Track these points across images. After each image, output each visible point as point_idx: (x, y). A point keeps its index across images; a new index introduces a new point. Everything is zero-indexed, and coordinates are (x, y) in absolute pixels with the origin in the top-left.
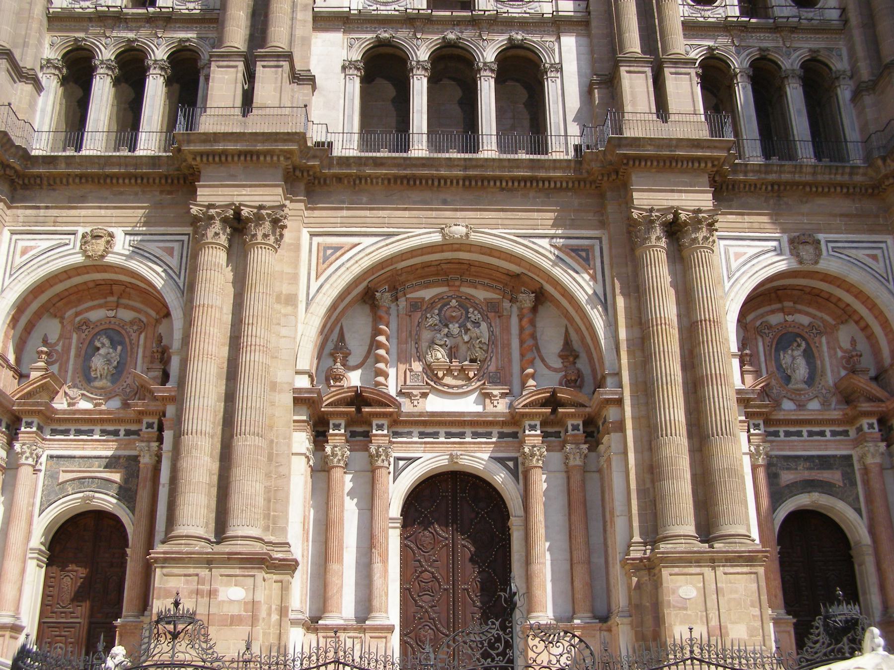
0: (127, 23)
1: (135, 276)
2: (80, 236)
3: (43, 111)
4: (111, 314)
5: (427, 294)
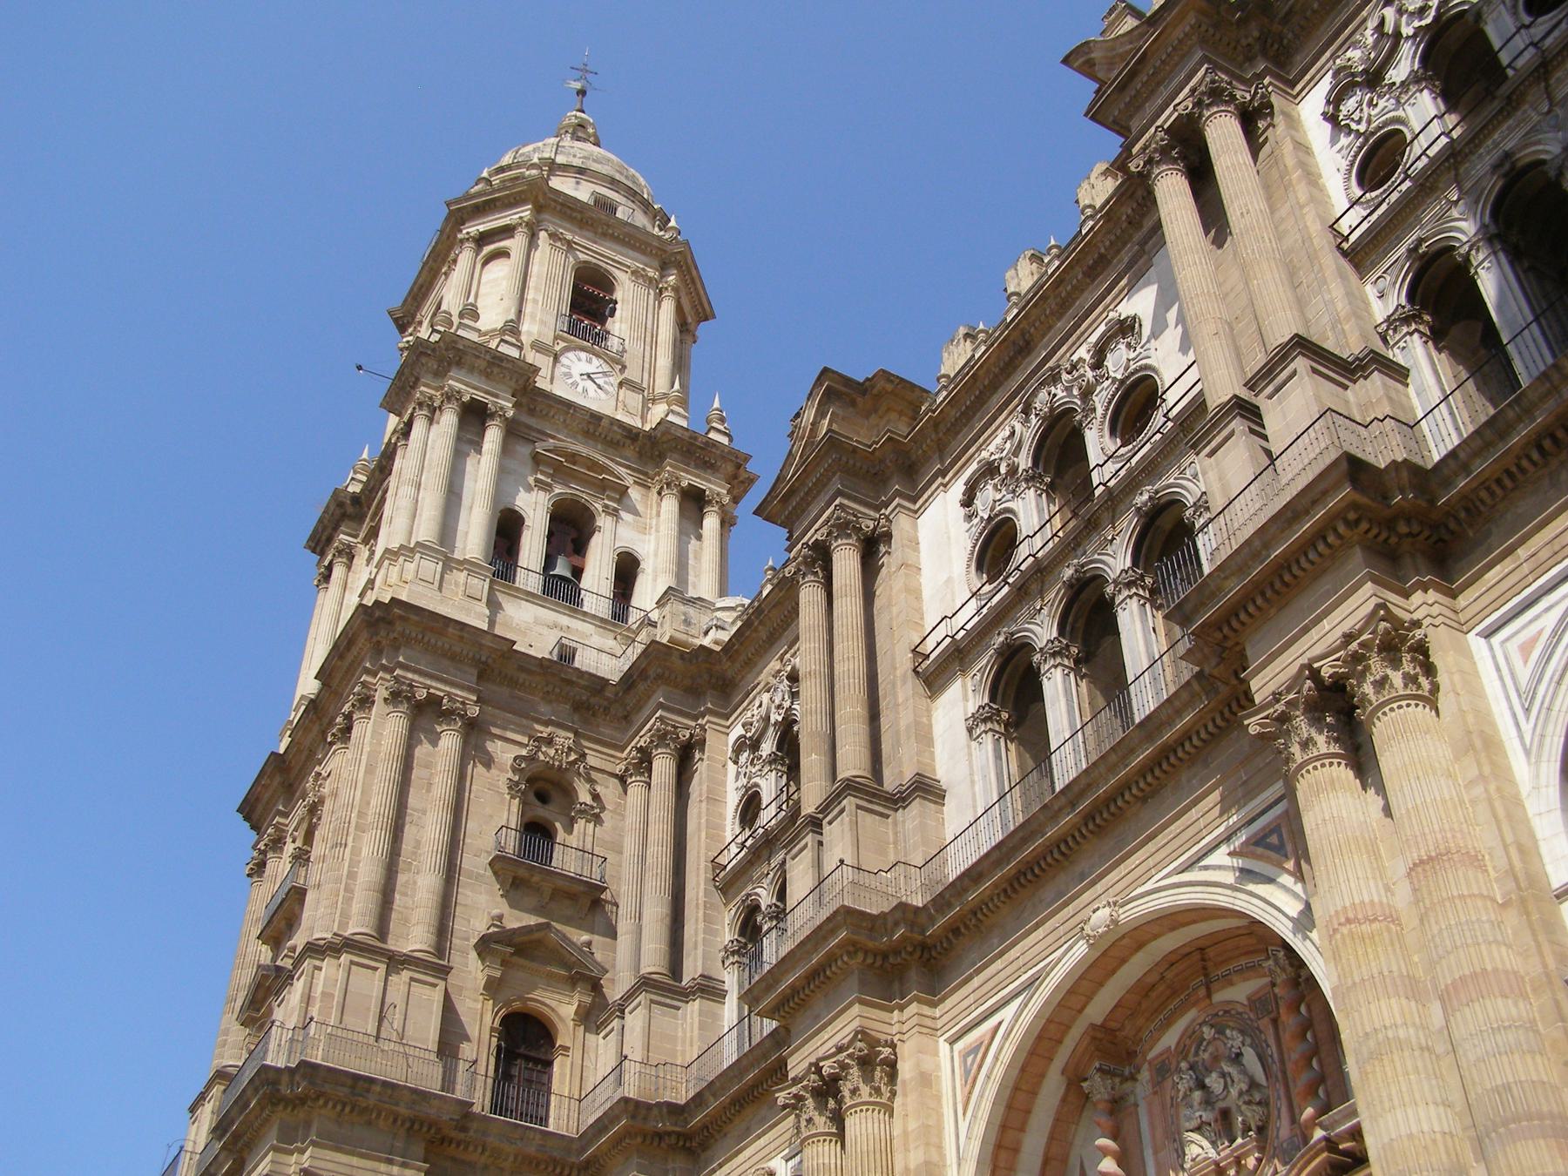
5: (1170, 1039)
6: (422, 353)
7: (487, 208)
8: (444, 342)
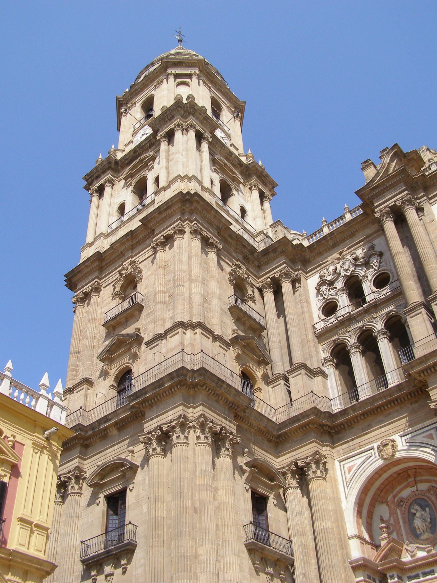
0: (356, 319)
1: (417, 460)
2: (376, 448)
3: (332, 387)
4: (414, 489)
6: (179, 106)
7: (179, 65)
8: (190, 104)
